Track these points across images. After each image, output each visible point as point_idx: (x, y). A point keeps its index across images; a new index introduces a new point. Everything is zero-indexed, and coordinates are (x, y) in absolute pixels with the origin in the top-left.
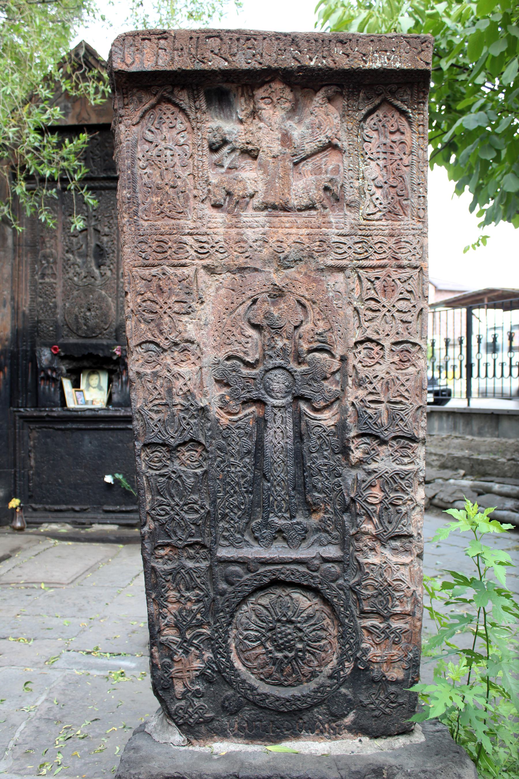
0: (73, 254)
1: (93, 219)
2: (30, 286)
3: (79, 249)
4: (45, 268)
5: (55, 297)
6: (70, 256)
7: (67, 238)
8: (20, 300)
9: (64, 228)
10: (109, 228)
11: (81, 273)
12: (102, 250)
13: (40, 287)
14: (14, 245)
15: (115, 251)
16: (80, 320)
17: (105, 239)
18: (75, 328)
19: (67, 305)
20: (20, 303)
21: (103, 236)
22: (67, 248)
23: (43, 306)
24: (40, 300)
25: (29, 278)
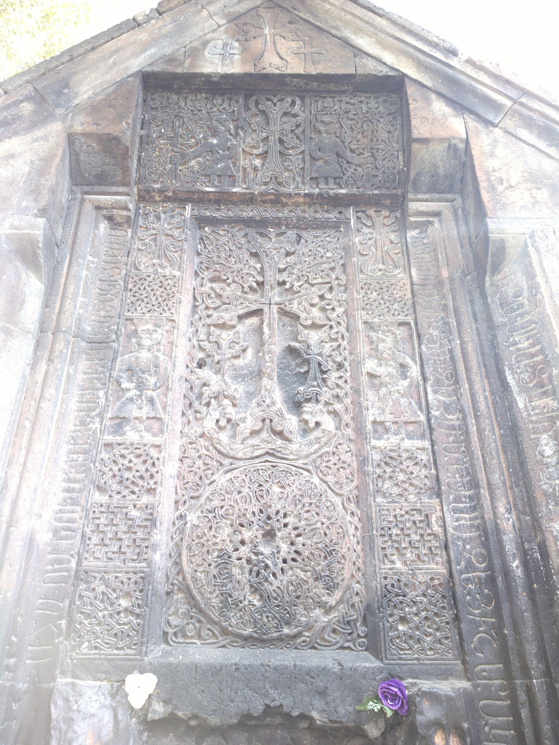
0: (218, 372)
1: (277, 290)
2: (70, 452)
3: (237, 357)
4: (131, 400)
5: (151, 491)
6: (206, 373)
7: (202, 331)
8: (25, 491)
9: (195, 307)
10: (323, 310)
11: (244, 420)
12: (307, 362)
13: (105, 455)
14: (42, 330)
15: (347, 364)
16: (235, 571)
17: (314, 337)
18: (215, 602)
19: (192, 518)
20: (21, 502)
21: (305, 327)
22: (201, 355)
23: (103, 520)
24: (99, 498)
25: (70, 425)
